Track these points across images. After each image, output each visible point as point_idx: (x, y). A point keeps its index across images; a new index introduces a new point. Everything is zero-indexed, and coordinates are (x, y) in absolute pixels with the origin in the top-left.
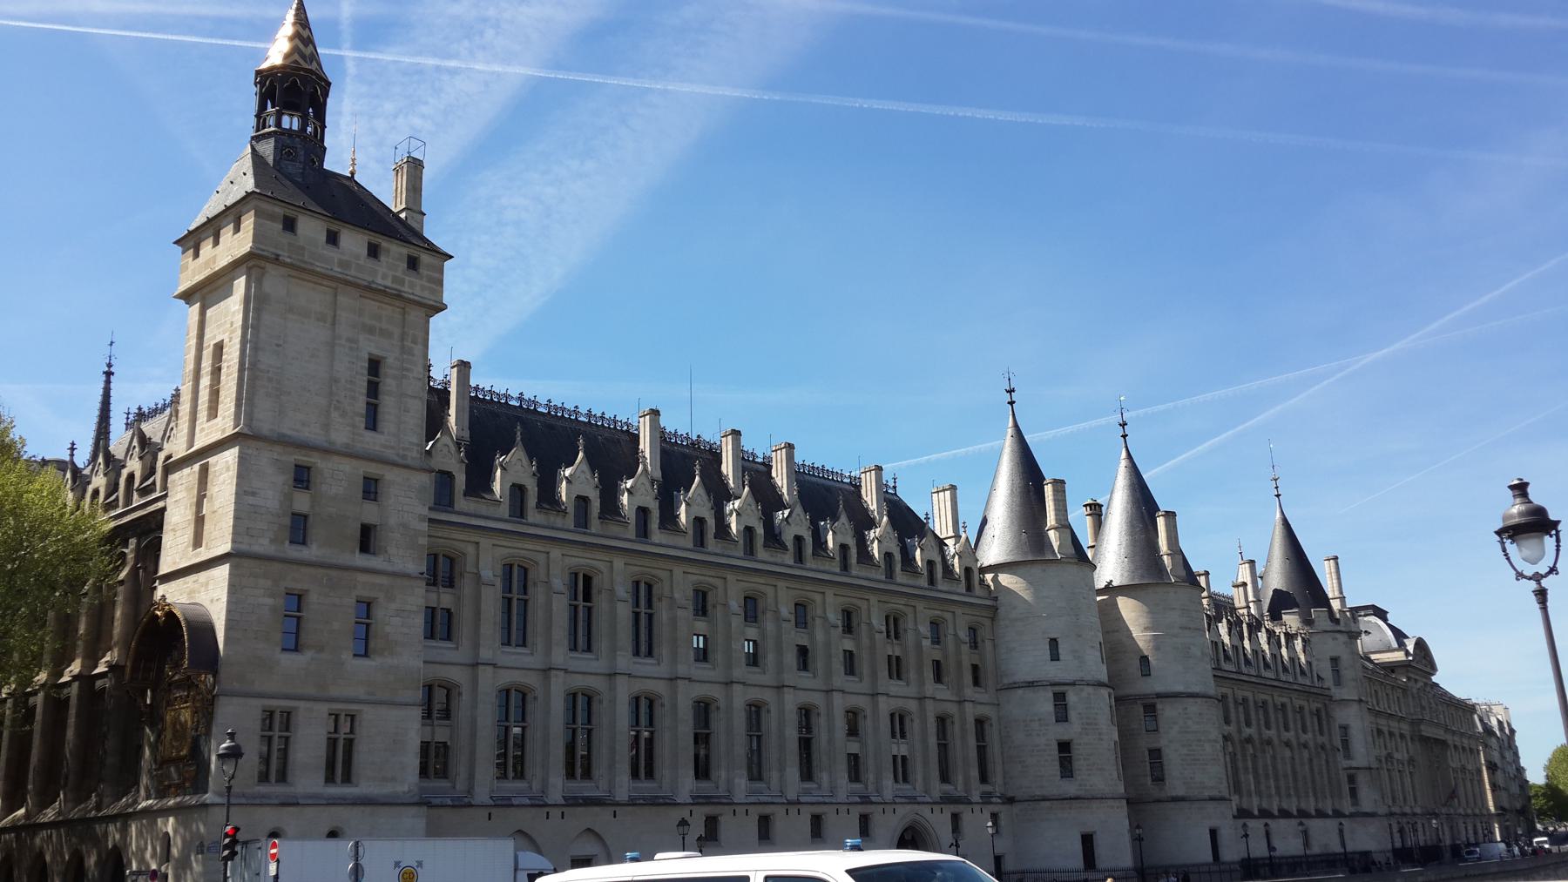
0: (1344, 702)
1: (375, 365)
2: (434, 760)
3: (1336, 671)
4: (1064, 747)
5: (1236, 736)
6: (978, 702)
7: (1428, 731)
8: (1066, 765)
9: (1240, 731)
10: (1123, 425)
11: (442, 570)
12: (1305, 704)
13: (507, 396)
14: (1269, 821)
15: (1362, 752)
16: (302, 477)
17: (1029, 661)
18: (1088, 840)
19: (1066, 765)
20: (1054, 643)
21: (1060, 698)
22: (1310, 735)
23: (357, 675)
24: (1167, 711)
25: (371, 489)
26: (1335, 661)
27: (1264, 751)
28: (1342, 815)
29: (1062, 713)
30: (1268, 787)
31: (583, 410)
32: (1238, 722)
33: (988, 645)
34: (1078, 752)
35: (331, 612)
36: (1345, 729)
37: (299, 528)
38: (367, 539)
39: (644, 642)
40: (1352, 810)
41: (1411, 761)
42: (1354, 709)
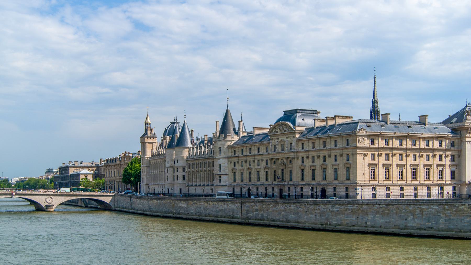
14: (196, 187)
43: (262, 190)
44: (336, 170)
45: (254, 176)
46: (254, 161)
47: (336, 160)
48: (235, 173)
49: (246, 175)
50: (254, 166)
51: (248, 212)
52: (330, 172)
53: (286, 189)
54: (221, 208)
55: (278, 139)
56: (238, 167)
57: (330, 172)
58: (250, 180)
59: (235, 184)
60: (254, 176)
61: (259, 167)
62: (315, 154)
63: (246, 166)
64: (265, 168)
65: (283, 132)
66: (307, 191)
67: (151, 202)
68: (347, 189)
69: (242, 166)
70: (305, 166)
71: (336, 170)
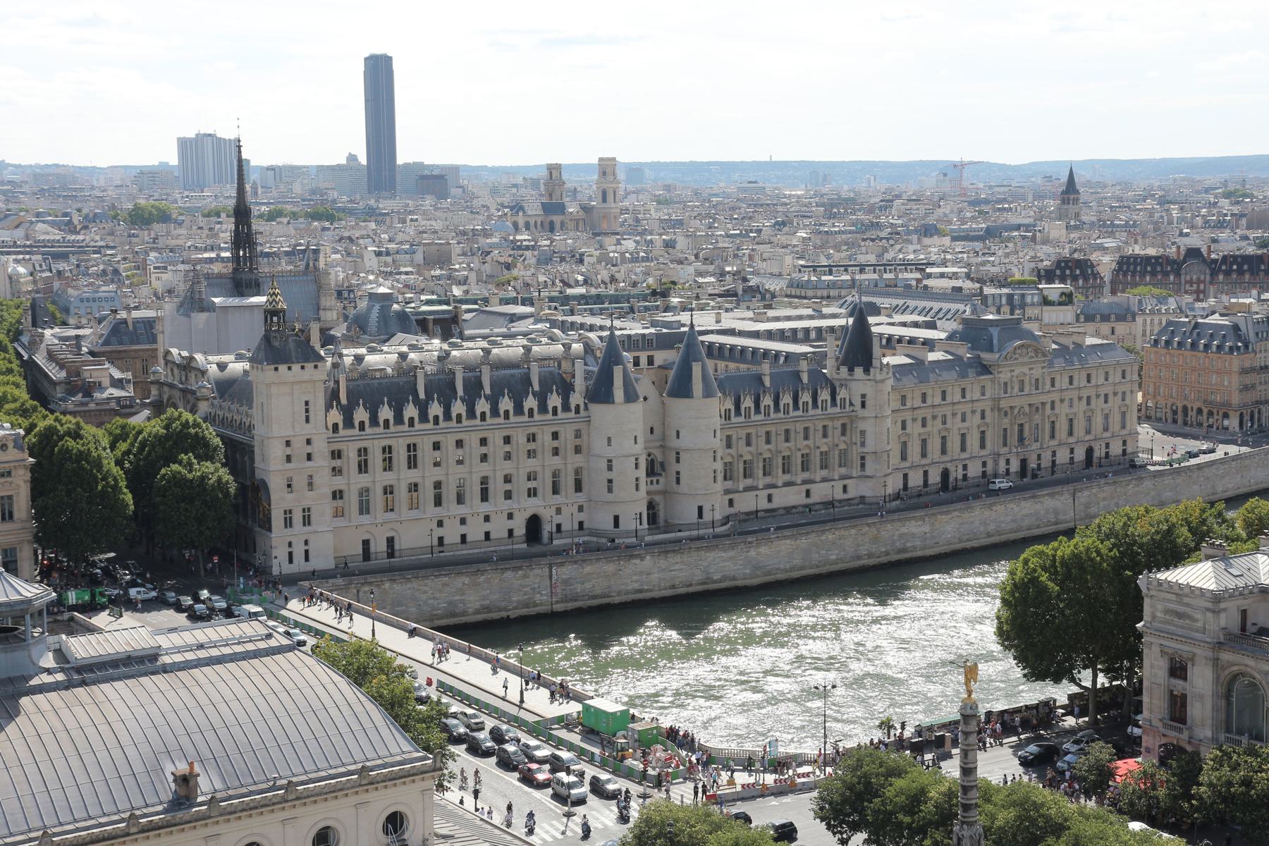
0: (863, 418)
1: (307, 403)
2: (339, 513)
4: (610, 481)
6: (578, 460)
7: (1003, 404)
8: (610, 490)
11: (336, 455)
12: (830, 423)
16: (288, 443)
17: (599, 445)
18: (616, 519)
19: (610, 490)
20: (609, 439)
21: (610, 461)
22: (830, 439)
23: (309, 499)
24: (682, 456)
25: (309, 442)
29: (610, 468)
33: (585, 437)
34: (614, 483)
35: (300, 482)
36: (863, 433)
37: (289, 459)
38: (309, 457)
39: (412, 463)
42: (873, 420)
43: (974, 470)
44: (1107, 417)
45: (954, 444)
46: (954, 415)
47: (1106, 402)
48: (904, 444)
49: (934, 446)
50: (955, 426)
51: (1087, 506)
52: (1098, 421)
53: (1034, 457)
54: (1025, 512)
56: (915, 429)
57: (1098, 421)
58: (944, 452)
59: (907, 464)
60: (954, 444)
61: (965, 424)
62: (1074, 394)
63: (934, 427)
65: (1026, 359)
66: (1063, 457)
67: (764, 549)
68: (1124, 443)
69: (924, 425)
70: (1057, 416)
71: (1107, 417)
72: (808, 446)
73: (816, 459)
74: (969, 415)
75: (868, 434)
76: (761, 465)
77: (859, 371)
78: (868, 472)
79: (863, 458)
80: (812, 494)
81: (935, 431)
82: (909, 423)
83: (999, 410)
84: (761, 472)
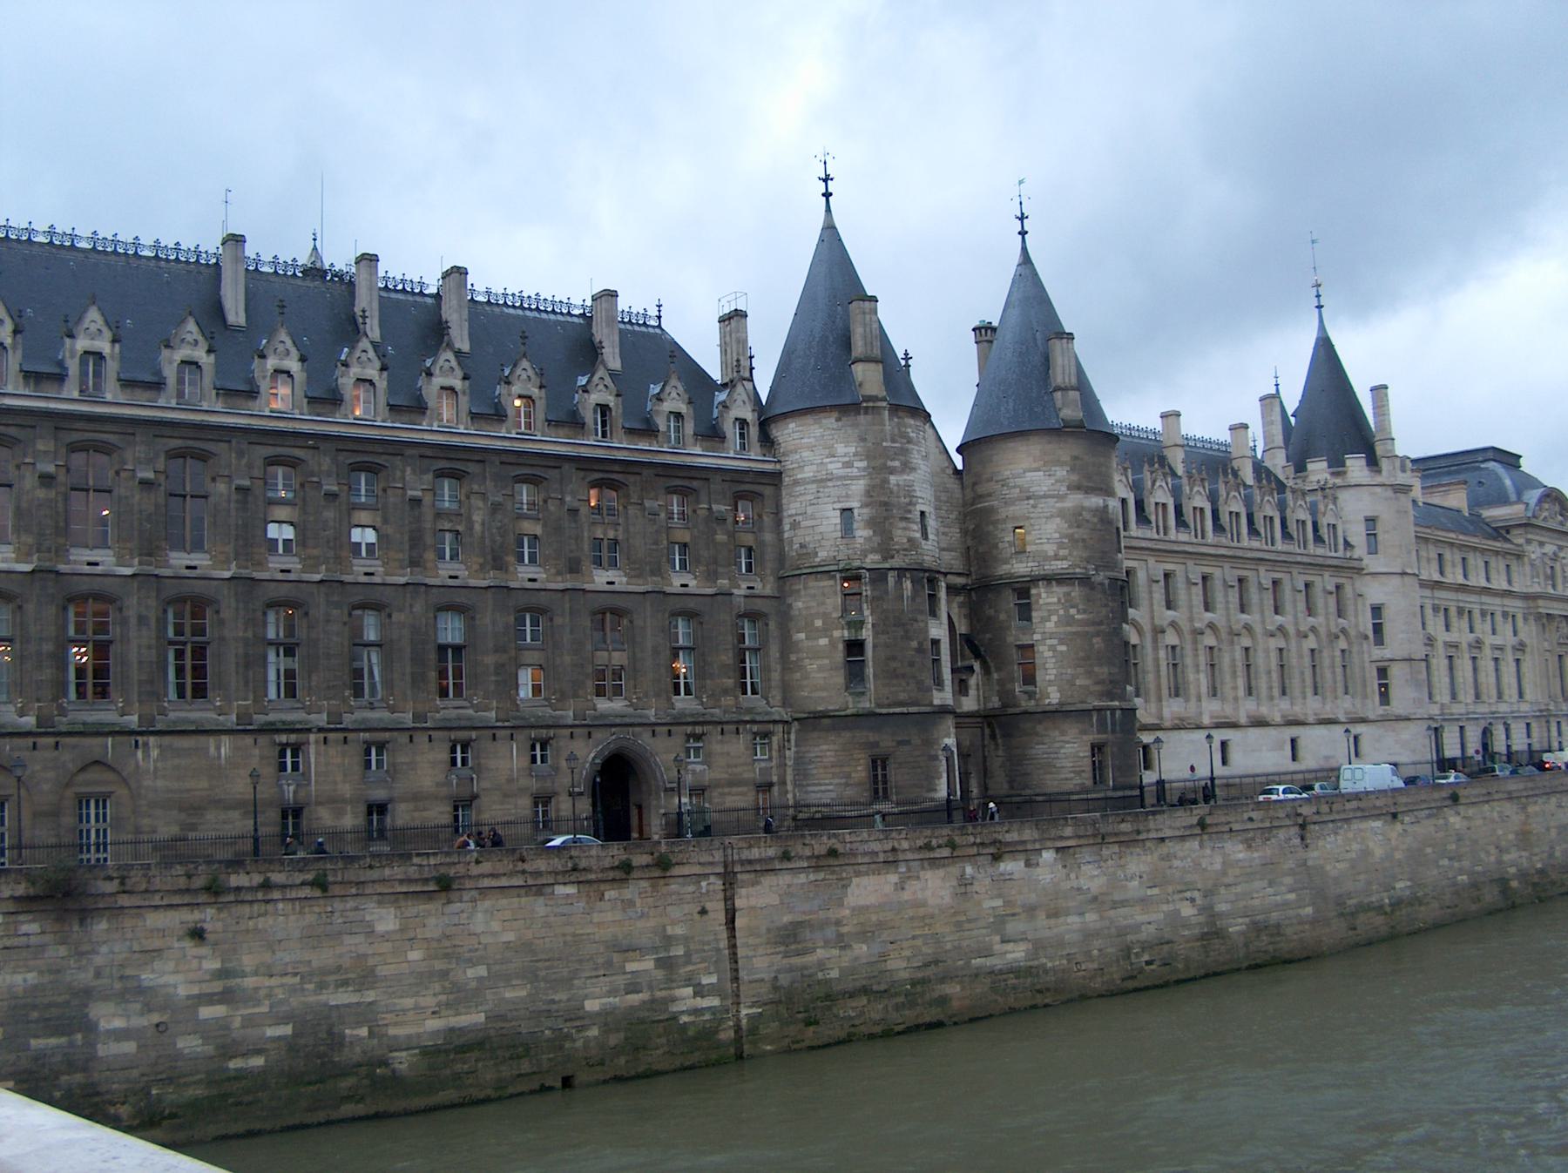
3: (1372, 536)
5: (1185, 626)
7: (1544, 607)
9: (1191, 619)
10: (1022, 218)
13: (30, 231)
15: (1401, 639)
20: (846, 511)
22: (1321, 619)
26: (1371, 521)
27: (1232, 643)
28: (1364, 721)
30: (1235, 688)
31: (147, 240)
32: (1190, 607)
36: (1377, 610)
40: (1381, 710)
41: (1520, 648)
42: (1396, 580)
55: (1542, 544)
64: (1514, 648)
72: (1281, 628)
73: (1299, 663)
74: (1498, 618)
75: (1386, 613)
76: (1203, 659)
77: (1356, 466)
78: (1398, 705)
79: (1382, 672)
80: (1301, 753)
81: (1464, 646)
82: (1429, 611)
83: (1539, 617)
84: (1198, 680)
